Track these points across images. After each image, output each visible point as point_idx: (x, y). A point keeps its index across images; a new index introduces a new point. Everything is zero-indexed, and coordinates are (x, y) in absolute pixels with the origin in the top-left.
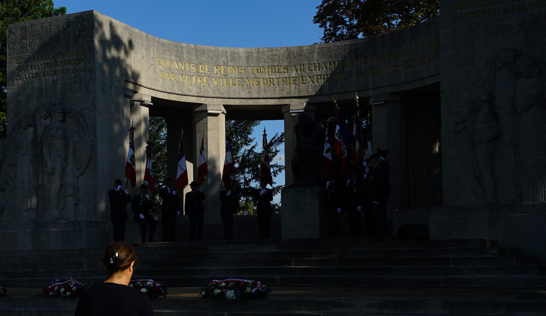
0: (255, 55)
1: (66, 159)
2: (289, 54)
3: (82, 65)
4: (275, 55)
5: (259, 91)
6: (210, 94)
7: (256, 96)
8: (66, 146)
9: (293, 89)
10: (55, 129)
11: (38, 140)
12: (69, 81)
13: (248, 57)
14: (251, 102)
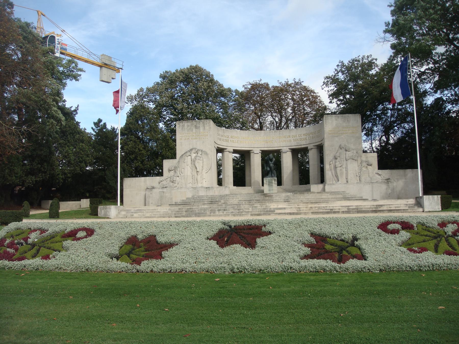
1: (203, 167)
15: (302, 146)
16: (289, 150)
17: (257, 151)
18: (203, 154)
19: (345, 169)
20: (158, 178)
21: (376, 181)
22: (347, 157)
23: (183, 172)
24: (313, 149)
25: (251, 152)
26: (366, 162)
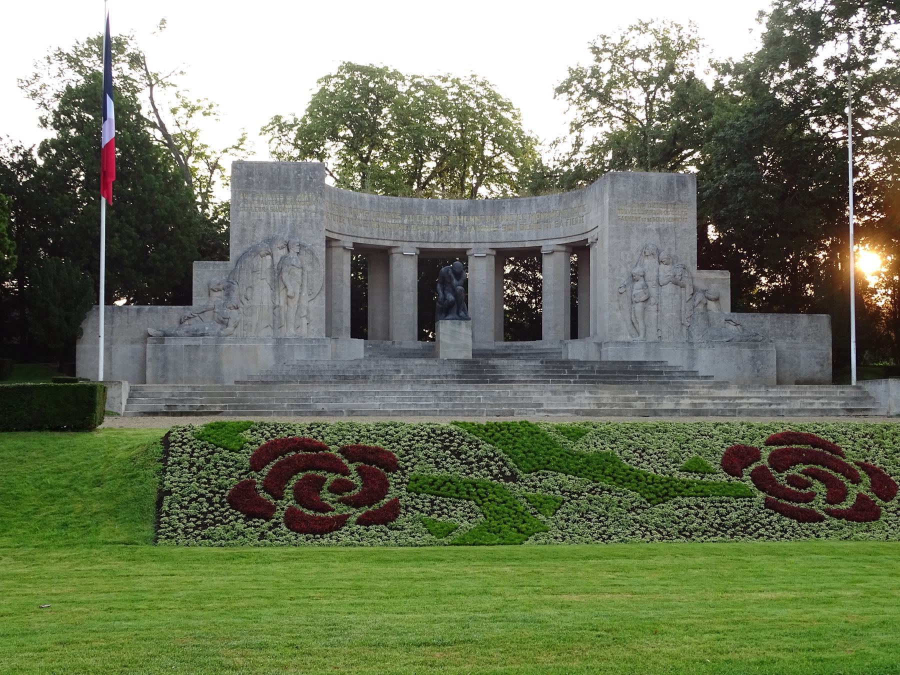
0: (376, 201)
2: (402, 204)
3: (313, 207)
4: (391, 203)
5: (379, 233)
6: (346, 233)
7: (377, 237)
8: (303, 274)
9: (405, 234)
10: (294, 260)
11: (276, 267)
12: (299, 219)
13: (371, 202)
14: (372, 242)
15: (527, 243)
16: (490, 252)
17: (410, 250)
18: (303, 252)
19: (655, 306)
20: (176, 311)
21: (728, 339)
22: (661, 278)
23: (249, 295)
24: (555, 253)
25: (393, 251)
26: (704, 291)
